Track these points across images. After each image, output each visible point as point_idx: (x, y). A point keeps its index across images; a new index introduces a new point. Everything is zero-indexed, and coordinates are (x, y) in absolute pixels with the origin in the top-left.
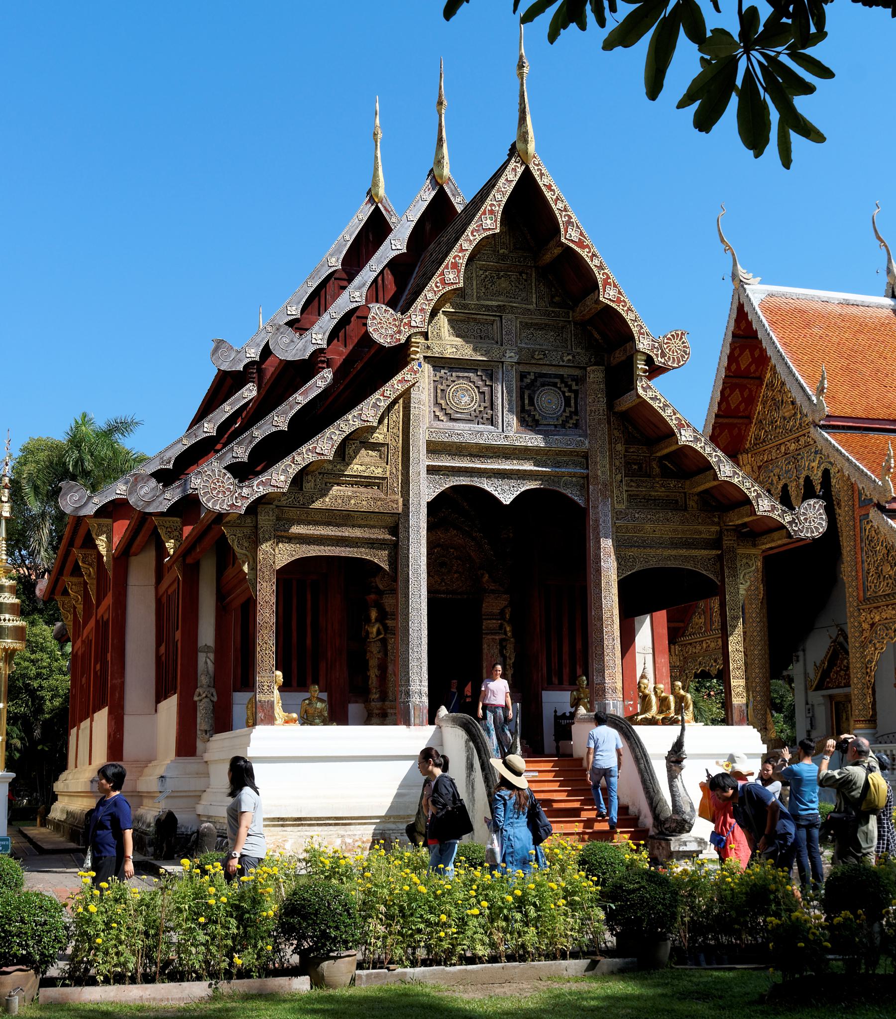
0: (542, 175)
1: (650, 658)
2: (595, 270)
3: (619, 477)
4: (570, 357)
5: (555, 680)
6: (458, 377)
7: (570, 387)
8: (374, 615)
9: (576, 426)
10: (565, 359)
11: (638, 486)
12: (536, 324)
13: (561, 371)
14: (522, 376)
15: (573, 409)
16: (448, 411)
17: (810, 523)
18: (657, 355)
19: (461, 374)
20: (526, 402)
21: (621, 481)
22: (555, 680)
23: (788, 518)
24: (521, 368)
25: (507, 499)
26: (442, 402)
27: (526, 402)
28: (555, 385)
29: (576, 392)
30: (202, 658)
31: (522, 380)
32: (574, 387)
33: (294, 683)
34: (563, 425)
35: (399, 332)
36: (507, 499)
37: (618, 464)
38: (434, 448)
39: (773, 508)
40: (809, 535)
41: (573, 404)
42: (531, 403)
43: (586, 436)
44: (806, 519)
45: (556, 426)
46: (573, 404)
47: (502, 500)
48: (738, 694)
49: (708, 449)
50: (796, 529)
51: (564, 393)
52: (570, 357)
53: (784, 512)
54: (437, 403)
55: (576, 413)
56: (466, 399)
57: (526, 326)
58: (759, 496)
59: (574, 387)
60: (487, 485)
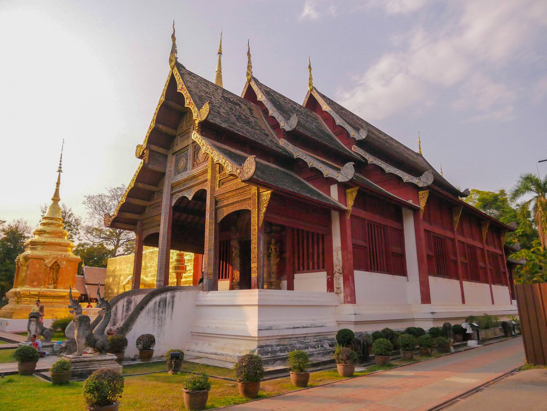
1: (340, 253)
5: (301, 268)
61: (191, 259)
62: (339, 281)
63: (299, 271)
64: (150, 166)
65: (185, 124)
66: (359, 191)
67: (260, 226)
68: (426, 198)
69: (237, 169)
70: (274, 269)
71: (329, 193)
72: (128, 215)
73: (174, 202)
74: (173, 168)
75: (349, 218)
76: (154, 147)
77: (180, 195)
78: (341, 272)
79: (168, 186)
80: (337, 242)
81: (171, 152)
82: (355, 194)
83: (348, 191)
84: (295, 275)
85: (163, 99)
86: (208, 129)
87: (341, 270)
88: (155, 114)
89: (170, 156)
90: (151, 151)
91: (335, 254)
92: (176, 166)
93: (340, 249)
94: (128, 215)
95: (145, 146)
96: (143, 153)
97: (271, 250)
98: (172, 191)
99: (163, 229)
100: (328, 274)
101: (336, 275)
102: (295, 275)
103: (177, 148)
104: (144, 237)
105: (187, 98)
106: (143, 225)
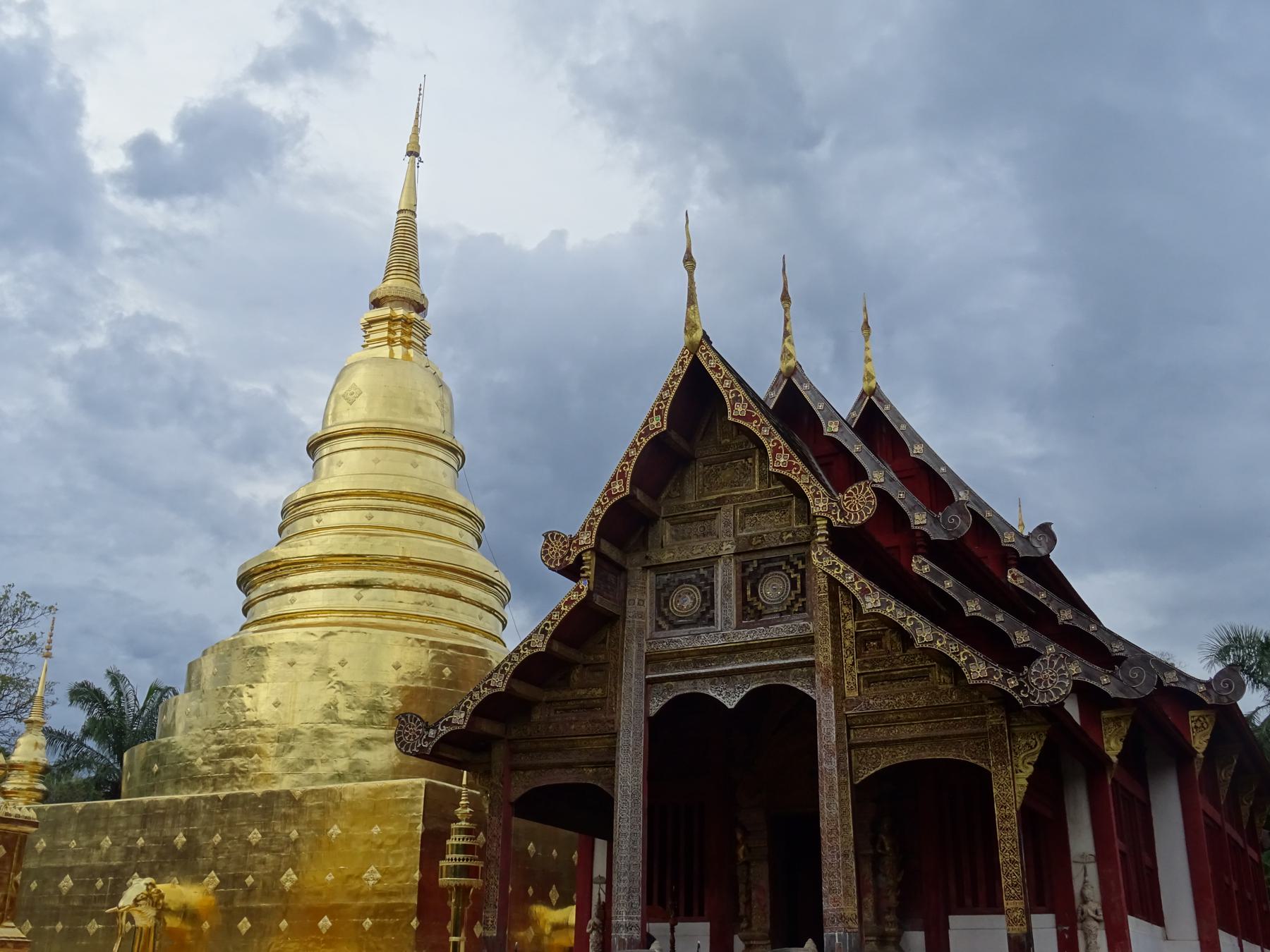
1: (1092, 869)
3: (849, 661)
4: (790, 535)
5: (968, 901)
7: (795, 567)
8: (739, 836)
9: (803, 609)
11: (873, 667)
13: (785, 553)
14: (744, 566)
15: (799, 591)
17: (1046, 684)
18: (835, 516)
20: (749, 593)
22: (968, 901)
23: (1013, 683)
24: (741, 558)
25: (731, 703)
27: (749, 593)
28: (780, 568)
29: (803, 572)
30: (596, 888)
31: (744, 571)
32: (801, 566)
34: (788, 612)
35: (569, 554)
36: (731, 703)
37: (848, 643)
38: (653, 660)
39: (991, 673)
40: (1045, 701)
42: (755, 592)
43: (811, 619)
44: (1039, 681)
45: (781, 613)
47: (727, 704)
49: (900, 614)
51: (789, 575)
52: (790, 535)
53: (1006, 676)
54: (660, 614)
55: (803, 594)
56: (689, 601)
58: (970, 660)
59: (801, 566)
61: (409, 836)
63: (963, 910)
65: (689, 490)
68: (1209, 730)
69: (1006, 676)
74: (648, 607)
76: (606, 547)
77: (686, 688)
79: (638, 657)
81: (637, 558)
84: (954, 920)
87: (1101, 913)
88: (628, 458)
89: (636, 574)
91: (1076, 870)
92: (662, 601)
93: (1093, 859)
94: (486, 727)
95: (587, 539)
96: (579, 561)
97: (883, 847)
100: (1059, 923)
102: (954, 920)
103: (667, 558)
104: (517, 793)
105: (776, 450)
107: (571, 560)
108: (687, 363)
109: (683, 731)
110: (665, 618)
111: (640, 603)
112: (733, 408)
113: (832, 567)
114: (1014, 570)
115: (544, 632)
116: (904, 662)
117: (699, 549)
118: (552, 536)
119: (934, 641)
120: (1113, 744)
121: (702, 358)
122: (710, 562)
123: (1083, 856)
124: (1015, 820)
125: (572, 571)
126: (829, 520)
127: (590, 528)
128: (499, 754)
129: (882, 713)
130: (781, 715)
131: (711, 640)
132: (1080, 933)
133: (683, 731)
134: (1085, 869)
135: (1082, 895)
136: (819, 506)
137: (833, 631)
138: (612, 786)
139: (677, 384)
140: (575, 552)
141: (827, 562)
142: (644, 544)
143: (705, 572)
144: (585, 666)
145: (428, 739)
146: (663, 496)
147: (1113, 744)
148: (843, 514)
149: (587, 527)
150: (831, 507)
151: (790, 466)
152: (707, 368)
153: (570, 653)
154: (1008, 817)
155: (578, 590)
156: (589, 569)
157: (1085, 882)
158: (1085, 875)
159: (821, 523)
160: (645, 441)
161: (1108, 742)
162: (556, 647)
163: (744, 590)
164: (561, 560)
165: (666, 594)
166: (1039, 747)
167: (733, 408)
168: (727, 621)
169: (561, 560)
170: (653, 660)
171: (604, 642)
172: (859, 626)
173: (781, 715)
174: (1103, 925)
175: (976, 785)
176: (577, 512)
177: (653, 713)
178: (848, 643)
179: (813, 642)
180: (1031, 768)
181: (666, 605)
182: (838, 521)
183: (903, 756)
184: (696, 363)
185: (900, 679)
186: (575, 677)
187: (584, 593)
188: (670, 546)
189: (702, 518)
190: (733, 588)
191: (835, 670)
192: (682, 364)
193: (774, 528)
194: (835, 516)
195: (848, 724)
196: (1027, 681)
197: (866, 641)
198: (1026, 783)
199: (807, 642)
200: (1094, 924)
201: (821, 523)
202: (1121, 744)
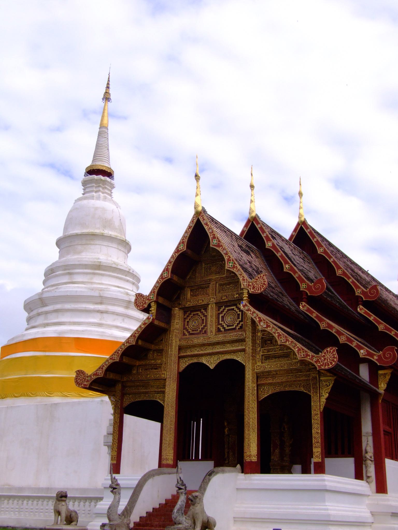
0: (204, 219)
1: (370, 439)
2: (224, 255)
3: (259, 349)
6: (194, 315)
8: (226, 424)
10: (235, 297)
11: (268, 352)
12: (226, 283)
16: (189, 330)
17: (327, 360)
18: (250, 289)
19: (195, 313)
21: (260, 351)
26: (187, 327)
33: (275, 457)
35: (145, 303)
37: (258, 342)
41: (240, 317)
43: (245, 331)
44: (325, 359)
46: (240, 317)
47: (210, 367)
48: (317, 456)
50: (319, 365)
52: (237, 295)
57: (220, 285)
60: (204, 361)
62: (371, 470)
64: (156, 322)
66: (392, 374)
67: (321, 410)
70: (287, 450)
71: (358, 372)
72: (111, 376)
73: (183, 365)
75: (380, 401)
76: (161, 300)
77: (195, 360)
78: (373, 459)
80: (367, 427)
82: (388, 377)
83: (380, 372)
85: (183, 248)
86: (258, 301)
87: (373, 457)
90: (159, 306)
91: (364, 439)
93: (371, 434)
94: (111, 376)
95: (154, 298)
96: (149, 306)
98: (179, 353)
99: (170, 399)
101: (369, 462)
103: (188, 304)
106: (124, 387)
107: (146, 306)
108: (195, 221)
109: (193, 377)
110: (187, 330)
111: (177, 323)
112: (212, 240)
113: (248, 310)
114: (361, 307)
115: (134, 336)
116: (280, 350)
117: (201, 300)
118: (139, 295)
119: (286, 342)
120: (382, 385)
121: (201, 220)
122: (205, 307)
123: (367, 433)
124: (319, 416)
125: (146, 310)
126: (248, 291)
127: (154, 292)
128: (119, 387)
129: (270, 372)
130: (232, 372)
131: (207, 338)
132: (364, 466)
133: (193, 377)
134: (368, 439)
135: (366, 450)
136: (244, 284)
137: (253, 337)
138: (164, 401)
139: (190, 230)
140: (148, 302)
141: (246, 308)
142: (178, 298)
143: (203, 311)
144: (154, 350)
145: (88, 381)
146: (188, 277)
147: (382, 385)
148: (254, 288)
149: (152, 292)
150: (249, 285)
151: (234, 267)
152: (203, 224)
153: (147, 345)
154: (317, 414)
155: (148, 318)
156: (154, 308)
157: (367, 444)
158: (368, 441)
159: (245, 291)
160: (177, 255)
161: (381, 384)
162: (140, 342)
163: (218, 318)
164: (142, 306)
165: (188, 320)
166: (331, 386)
167: (212, 240)
168: (211, 332)
169: (142, 306)
170: (180, 349)
171: (162, 340)
172: (263, 335)
173: (232, 372)
174: (373, 462)
175: (304, 401)
176: (147, 286)
177: (181, 369)
178: (258, 342)
179: (245, 341)
180: (327, 394)
181: (188, 325)
182: (251, 291)
183: (278, 390)
184: (198, 221)
185: (279, 357)
186: (150, 355)
187: (151, 320)
188: (190, 300)
189: (202, 288)
190: (214, 317)
191: (253, 353)
192: (193, 221)
193: (229, 294)
194: (250, 289)
195: (258, 376)
196: (320, 358)
197: (266, 341)
198: (325, 400)
199: (243, 340)
200: (370, 462)
201: (245, 291)
202: (386, 385)
